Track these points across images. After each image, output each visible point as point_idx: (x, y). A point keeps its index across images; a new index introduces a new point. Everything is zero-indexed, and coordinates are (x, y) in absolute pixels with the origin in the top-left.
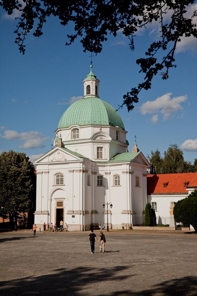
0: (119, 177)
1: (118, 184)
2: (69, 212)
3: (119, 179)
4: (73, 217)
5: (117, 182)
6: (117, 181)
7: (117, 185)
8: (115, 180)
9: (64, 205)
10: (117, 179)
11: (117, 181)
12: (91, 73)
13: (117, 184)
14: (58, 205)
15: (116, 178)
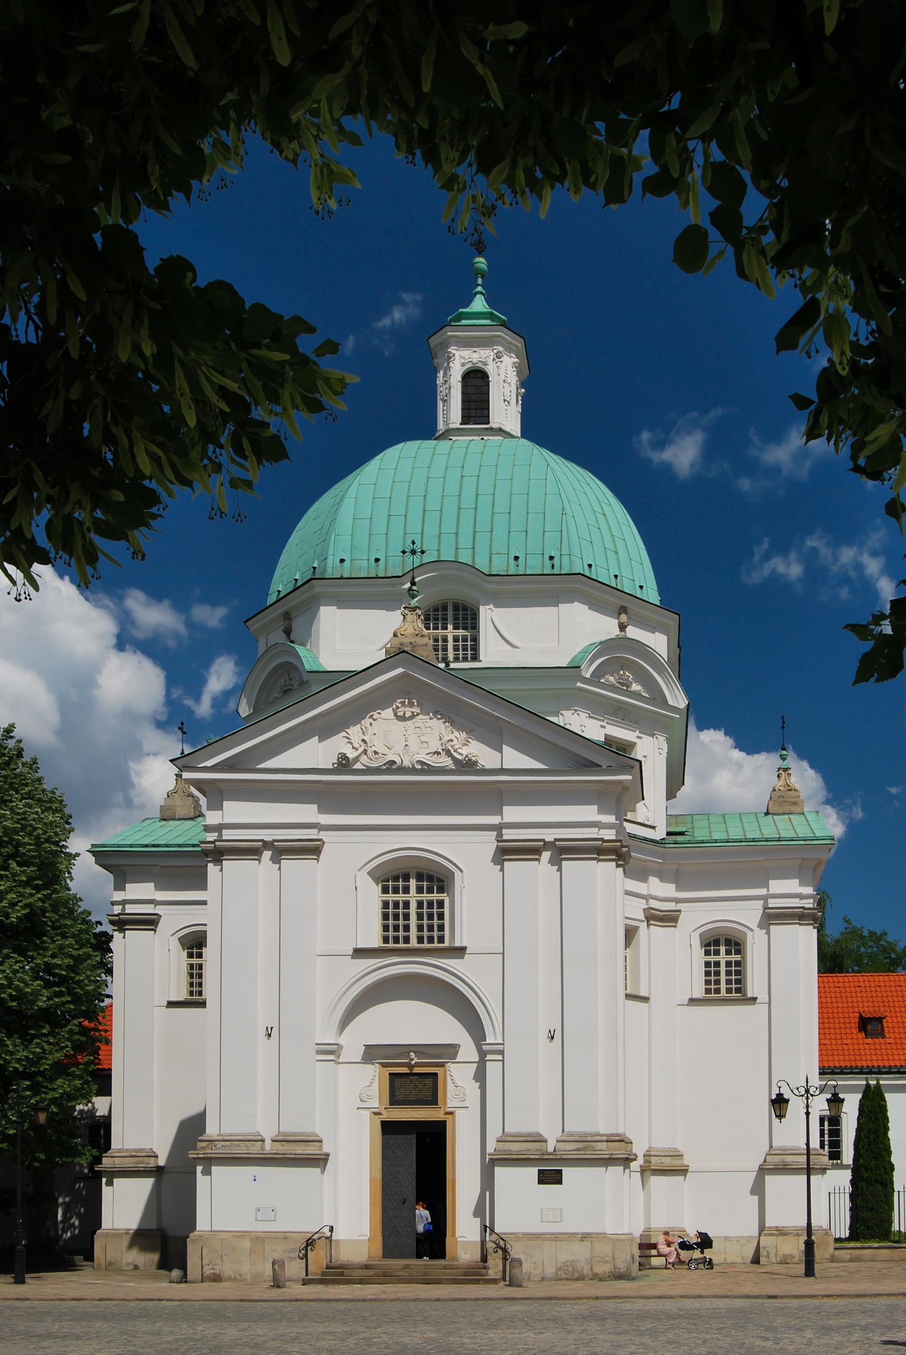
0: (735, 944)
1: (729, 991)
2: (516, 1147)
3: (734, 958)
4: (550, 1177)
5: (723, 977)
6: (723, 969)
7: (718, 991)
8: (707, 964)
9: (451, 1103)
10: (723, 958)
11: (723, 969)
12: (479, 304)
13: (723, 986)
14: (400, 1096)
15: (717, 953)
